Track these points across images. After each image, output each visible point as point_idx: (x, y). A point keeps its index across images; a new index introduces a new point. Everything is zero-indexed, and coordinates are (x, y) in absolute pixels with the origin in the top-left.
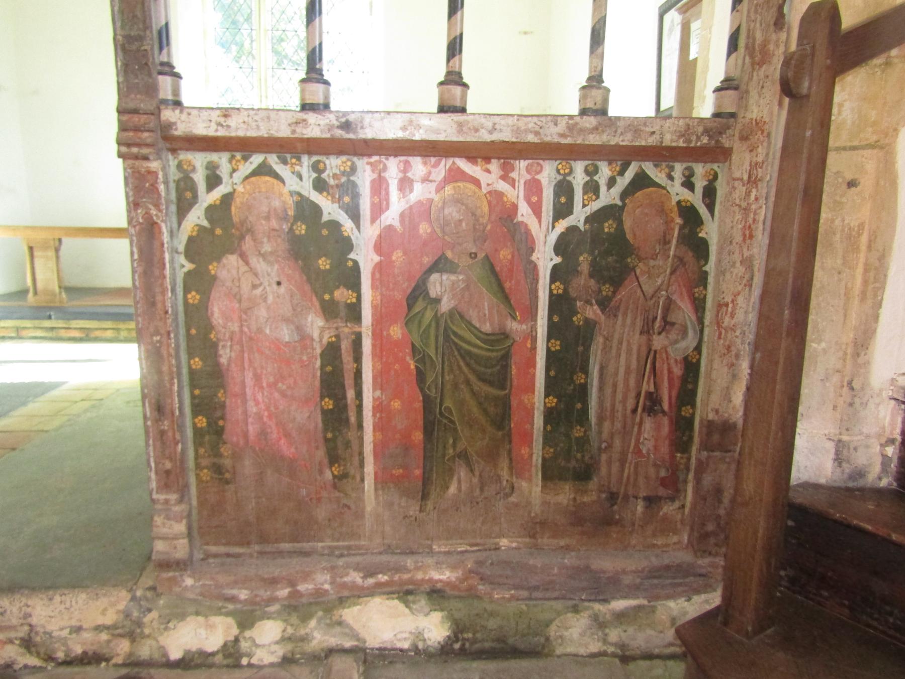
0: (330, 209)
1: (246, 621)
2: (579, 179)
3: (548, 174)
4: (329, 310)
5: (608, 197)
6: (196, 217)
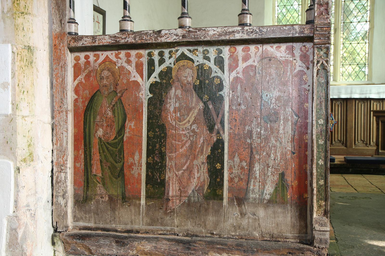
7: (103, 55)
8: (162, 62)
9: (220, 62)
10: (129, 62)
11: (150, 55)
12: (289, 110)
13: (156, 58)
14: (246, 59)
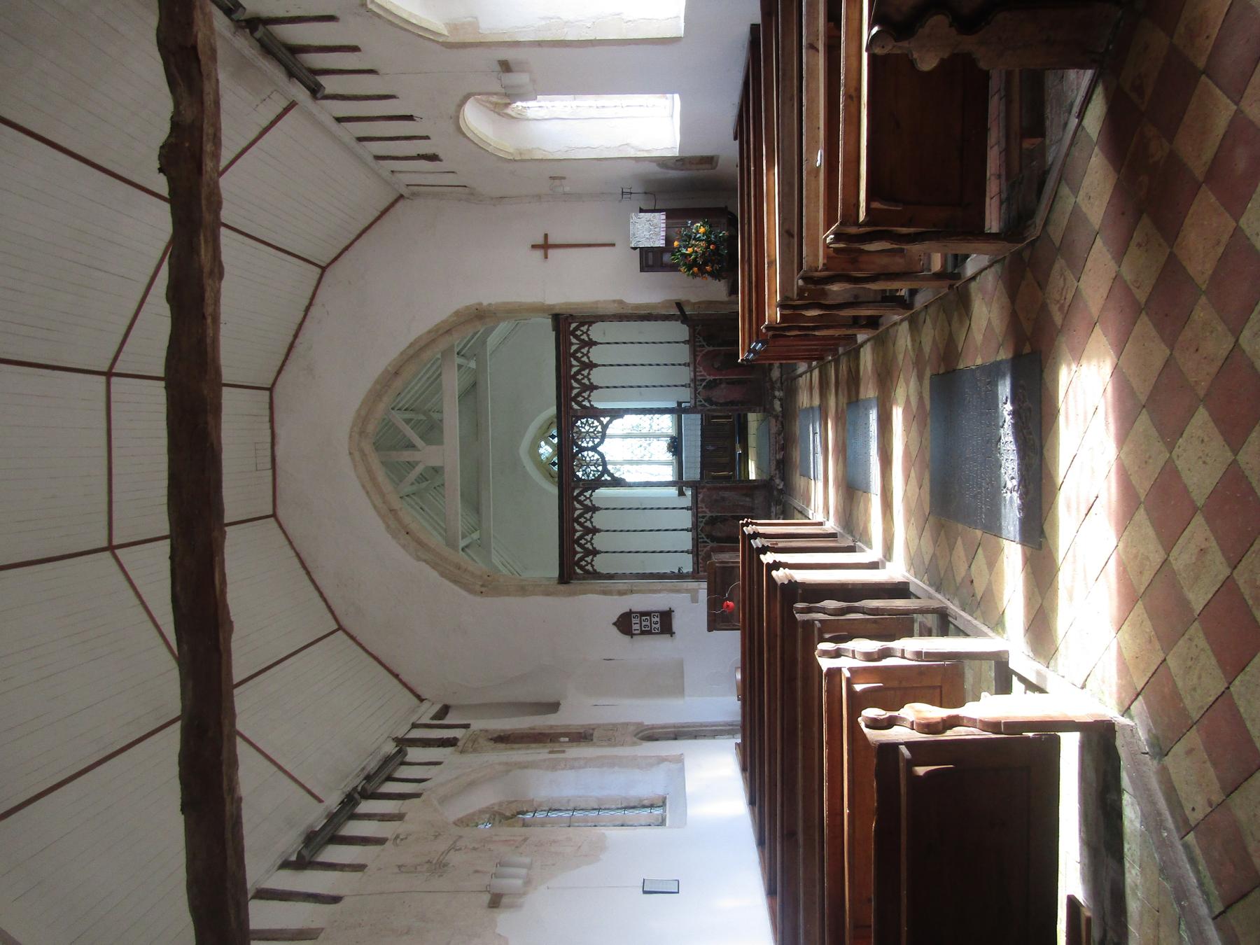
0: (704, 384)
1: (775, 397)
2: (698, 344)
3: (698, 349)
4: (721, 383)
5: (701, 339)
6: (706, 404)
7: (700, 561)
8: (703, 538)
9: (703, 517)
10: (703, 551)
11: (700, 543)
12: (720, 493)
13: (702, 540)
14: (702, 508)
